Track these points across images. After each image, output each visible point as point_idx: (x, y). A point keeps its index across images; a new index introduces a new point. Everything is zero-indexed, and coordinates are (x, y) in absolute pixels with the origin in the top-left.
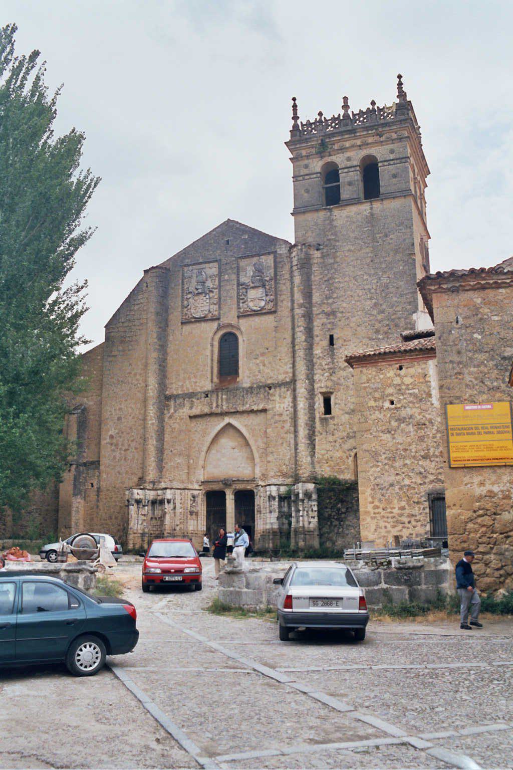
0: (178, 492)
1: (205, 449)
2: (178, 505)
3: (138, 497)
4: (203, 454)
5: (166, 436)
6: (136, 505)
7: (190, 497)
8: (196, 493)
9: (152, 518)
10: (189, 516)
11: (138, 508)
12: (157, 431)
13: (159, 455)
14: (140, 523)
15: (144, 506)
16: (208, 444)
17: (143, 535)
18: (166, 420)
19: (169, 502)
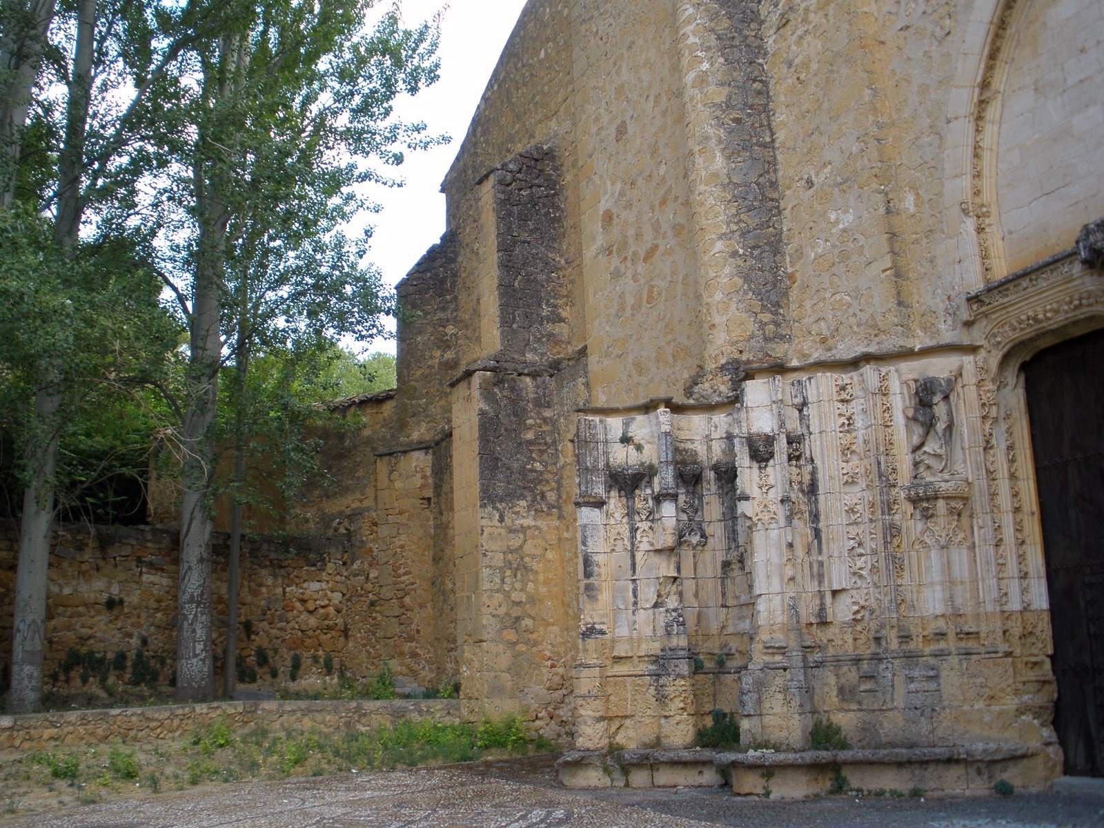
0: (822, 386)
1: (962, 99)
2: (830, 468)
3: (621, 456)
4: (962, 130)
5: (781, 117)
6: (615, 503)
7: (900, 403)
8: (940, 367)
9: (726, 565)
10: (913, 527)
11: (631, 513)
12: (729, 106)
13: (752, 221)
14: (648, 594)
15: (658, 499)
16: (970, 67)
17: (661, 662)
18: (770, 43)
19: (761, 451)
